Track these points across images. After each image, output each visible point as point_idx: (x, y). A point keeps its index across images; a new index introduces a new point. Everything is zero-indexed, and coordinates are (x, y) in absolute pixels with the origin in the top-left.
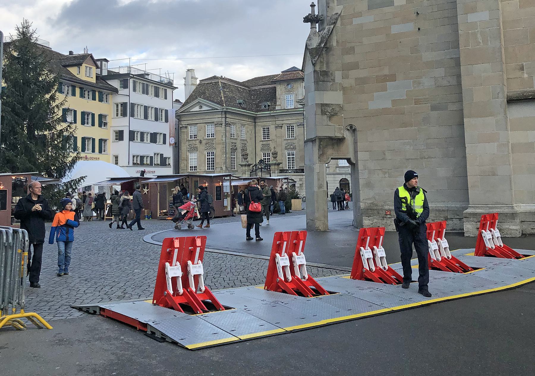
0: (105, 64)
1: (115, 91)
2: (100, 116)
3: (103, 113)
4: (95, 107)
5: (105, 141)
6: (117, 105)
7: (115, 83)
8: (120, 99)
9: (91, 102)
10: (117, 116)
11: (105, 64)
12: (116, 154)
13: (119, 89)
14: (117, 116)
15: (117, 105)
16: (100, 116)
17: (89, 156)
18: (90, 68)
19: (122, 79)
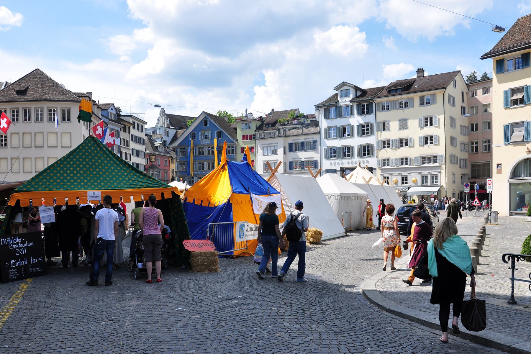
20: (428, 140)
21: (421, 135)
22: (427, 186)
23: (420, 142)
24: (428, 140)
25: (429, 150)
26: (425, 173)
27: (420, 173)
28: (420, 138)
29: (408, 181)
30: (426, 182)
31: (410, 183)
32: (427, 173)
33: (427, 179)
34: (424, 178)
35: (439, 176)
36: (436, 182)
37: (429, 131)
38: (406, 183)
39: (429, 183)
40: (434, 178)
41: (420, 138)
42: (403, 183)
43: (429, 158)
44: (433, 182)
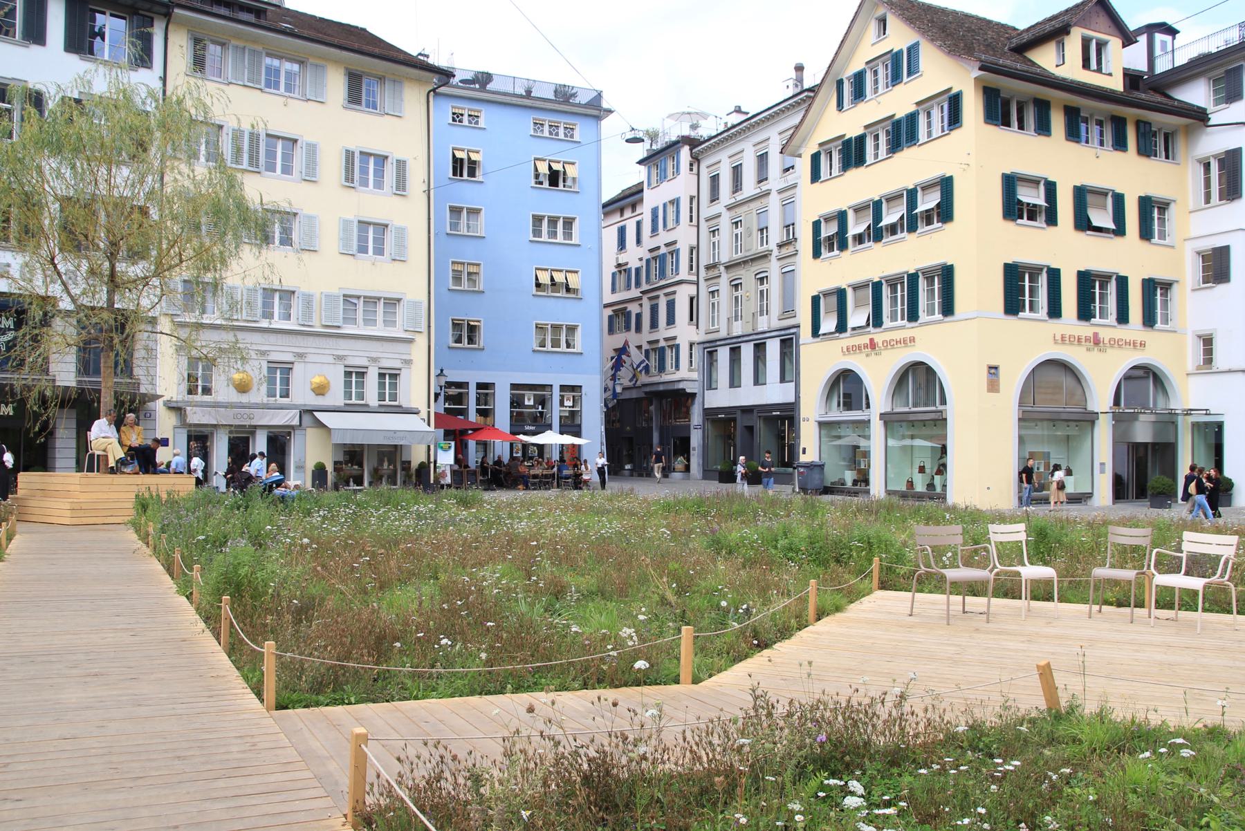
0: (1164, 43)
1: (1200, 117)
2: (1146, 204)
3: (1157, 191)
4: (1127, 173)
5: (1167, 286)
6: (1207, 166)
7: (1197, 94)
8: (1213, 143)
9: (1110, 157)
10: (1208, 200)
11: (1164, 43)
12: (1205, 329)
13: (1210, 108)
14: (1208, 200)
15: (1207, 166)
16: (1146, 204)
17: (1105, 334)
18: (1101, 46)
19: (1220, 72)
20: (371, 237)
21: (350, 216)
22: (365, 409)
23: (345, 240)
24: (371, 237)
25: (372, 276)
26: (358, 355)
27: (340, 358)
28: (346, 224)
29: (294, 388)
30: (361, 396)
31: (301, 395)
32: (364, 362)
33: (361, 385)
34: (355, 375)
35: (403, 373)
36: (394, 397)
37: (375, 204)
38: (286, 394)
39: (372, 398)
40: (390, 377)
41: (346, 224)
42: (271, 394)
43: (371, 301)
44: (382, 397)
